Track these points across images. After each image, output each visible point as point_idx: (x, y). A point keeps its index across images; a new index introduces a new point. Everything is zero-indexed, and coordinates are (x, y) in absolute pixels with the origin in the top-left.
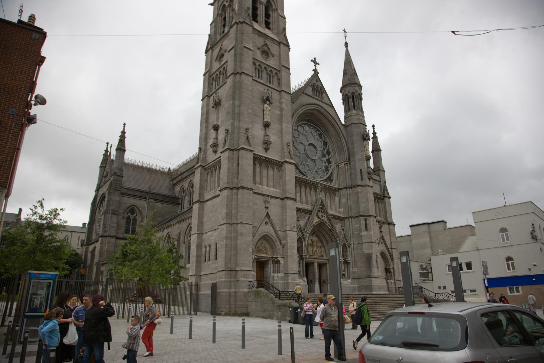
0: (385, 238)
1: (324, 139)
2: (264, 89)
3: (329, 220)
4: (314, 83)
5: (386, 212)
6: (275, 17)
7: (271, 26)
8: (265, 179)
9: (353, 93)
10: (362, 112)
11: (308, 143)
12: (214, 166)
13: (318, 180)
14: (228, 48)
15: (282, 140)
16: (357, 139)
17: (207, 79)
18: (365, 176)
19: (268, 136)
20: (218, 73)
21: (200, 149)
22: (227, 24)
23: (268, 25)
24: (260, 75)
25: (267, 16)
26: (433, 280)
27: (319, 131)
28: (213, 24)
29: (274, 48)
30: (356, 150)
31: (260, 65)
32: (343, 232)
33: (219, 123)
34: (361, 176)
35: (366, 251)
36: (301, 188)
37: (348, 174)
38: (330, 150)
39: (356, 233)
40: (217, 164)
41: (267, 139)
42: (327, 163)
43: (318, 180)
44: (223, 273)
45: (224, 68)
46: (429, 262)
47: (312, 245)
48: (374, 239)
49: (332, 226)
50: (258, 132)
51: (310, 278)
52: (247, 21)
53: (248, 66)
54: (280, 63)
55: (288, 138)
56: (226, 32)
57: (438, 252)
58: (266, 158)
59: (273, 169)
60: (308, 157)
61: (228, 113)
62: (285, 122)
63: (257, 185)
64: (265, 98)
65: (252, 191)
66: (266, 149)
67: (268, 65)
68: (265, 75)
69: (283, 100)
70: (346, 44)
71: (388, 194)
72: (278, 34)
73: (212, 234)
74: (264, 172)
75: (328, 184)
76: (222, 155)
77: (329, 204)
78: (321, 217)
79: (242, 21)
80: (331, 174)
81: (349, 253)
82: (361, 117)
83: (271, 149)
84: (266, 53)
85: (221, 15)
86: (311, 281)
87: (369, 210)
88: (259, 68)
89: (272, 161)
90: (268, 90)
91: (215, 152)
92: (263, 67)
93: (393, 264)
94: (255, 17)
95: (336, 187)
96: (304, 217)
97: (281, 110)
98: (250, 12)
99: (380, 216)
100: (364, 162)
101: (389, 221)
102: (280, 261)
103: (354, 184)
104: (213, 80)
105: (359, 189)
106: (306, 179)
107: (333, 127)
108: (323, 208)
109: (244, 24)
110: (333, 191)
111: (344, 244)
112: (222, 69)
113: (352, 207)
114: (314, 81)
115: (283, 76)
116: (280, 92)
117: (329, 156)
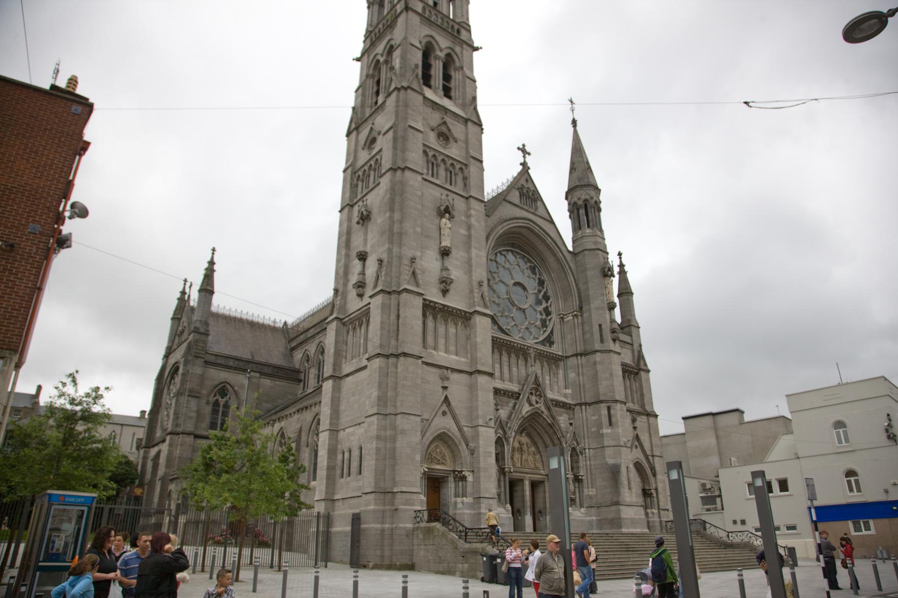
0: (642, 438)
1: (540, 275)
2: (442, 194)
3: (548, 409)
4: (522, 185)
5: (642, 395)
6: (459, 80)
7: (452, 94)
8: (442, 341)
9: (586, 200)
10: (601, 230)
11: (513, 282)
12: (359, 318)
13: (529, 342)
14: (384, 127)
15: (470, 276)
16: (593, 274)
17: (349, 177)
18: (608, 336)
19: (448, 270)
20: (366, 168)
21: (336, 291)
22: (382, 90)
23: (447, 92)
24: (435, 172)
25: (447, 77)
26: (723, 509)
27: (530, 261)
28: (360, 91)
29: (457, 129)
30: (591, 292)
31: (434, 156)
32: (571, 428)
33: (368, 249)
34: (601, 335)
35: (610, 461)
36: (501, 355)
37: (578, 333)
38: (550, 293)
39: (593, 429)
40: (364, 316)
41: (445, 275)
42: (544, 315)
43: (530, 342)
44: (371, 496)
45: (377, 160)
46: (716, 479)
47: (521, 450)
48: (623, 440)
49: (553, 418)
50: (430, 263)
51: (517, 505)
52: (415, 85)
53: (415, 158)
54: (467, 152)
55: (480, 273)
56: (380, 102)
57: (731, 462)
58: (444, 306)
59: (456, 324)
60: (513, 304)
61: (382, 233)
62: (475, 248)
63: (429, 350)
64: (442, 208)
65: (420, 361)
66: (445, 292)
67: (447, 156)
68: (442, 172)
69: (473, 212)
70: (574, 122)
71: (646, 365)
72: (463, 106)
73: (354, 431)
74: (441, 330)
75: (546, 349)
76: (372, 301)
77: (547, 382)
78: (534, 403)
79: (405, 86)
80: (552, 332)
81: (581, 464)
82: (599, 240)
83: (452, 292)
84: (445, 136)
85: (373, 76)
86: (519, 511)
87: (614, 392)
88: (432, 160)
89: (455, 311)
90: (447, 195)
91: (361, 296)
92: (440, 158)
93: (656, 483)
94: (427, 79)
95: (560, 353)
96: (507, 403)
97: (469, 227)
98: (420, 71)
99: (633, 403)
100: (606, 313)
101: (648, 410)
102: (466, 477)
103: (589, 348)
104: (358, 180)
105: (598, 357)
106: (509, 341)
107: (555, 255)
108: (538, 388)
109: (409, 91)
110: (553, 361)
111: (574, 449)
112: (372, 162)
113: (587, 387)
114: (523, 181)
115: (471, 174)
116: (467, 198)
117: (547, 302)
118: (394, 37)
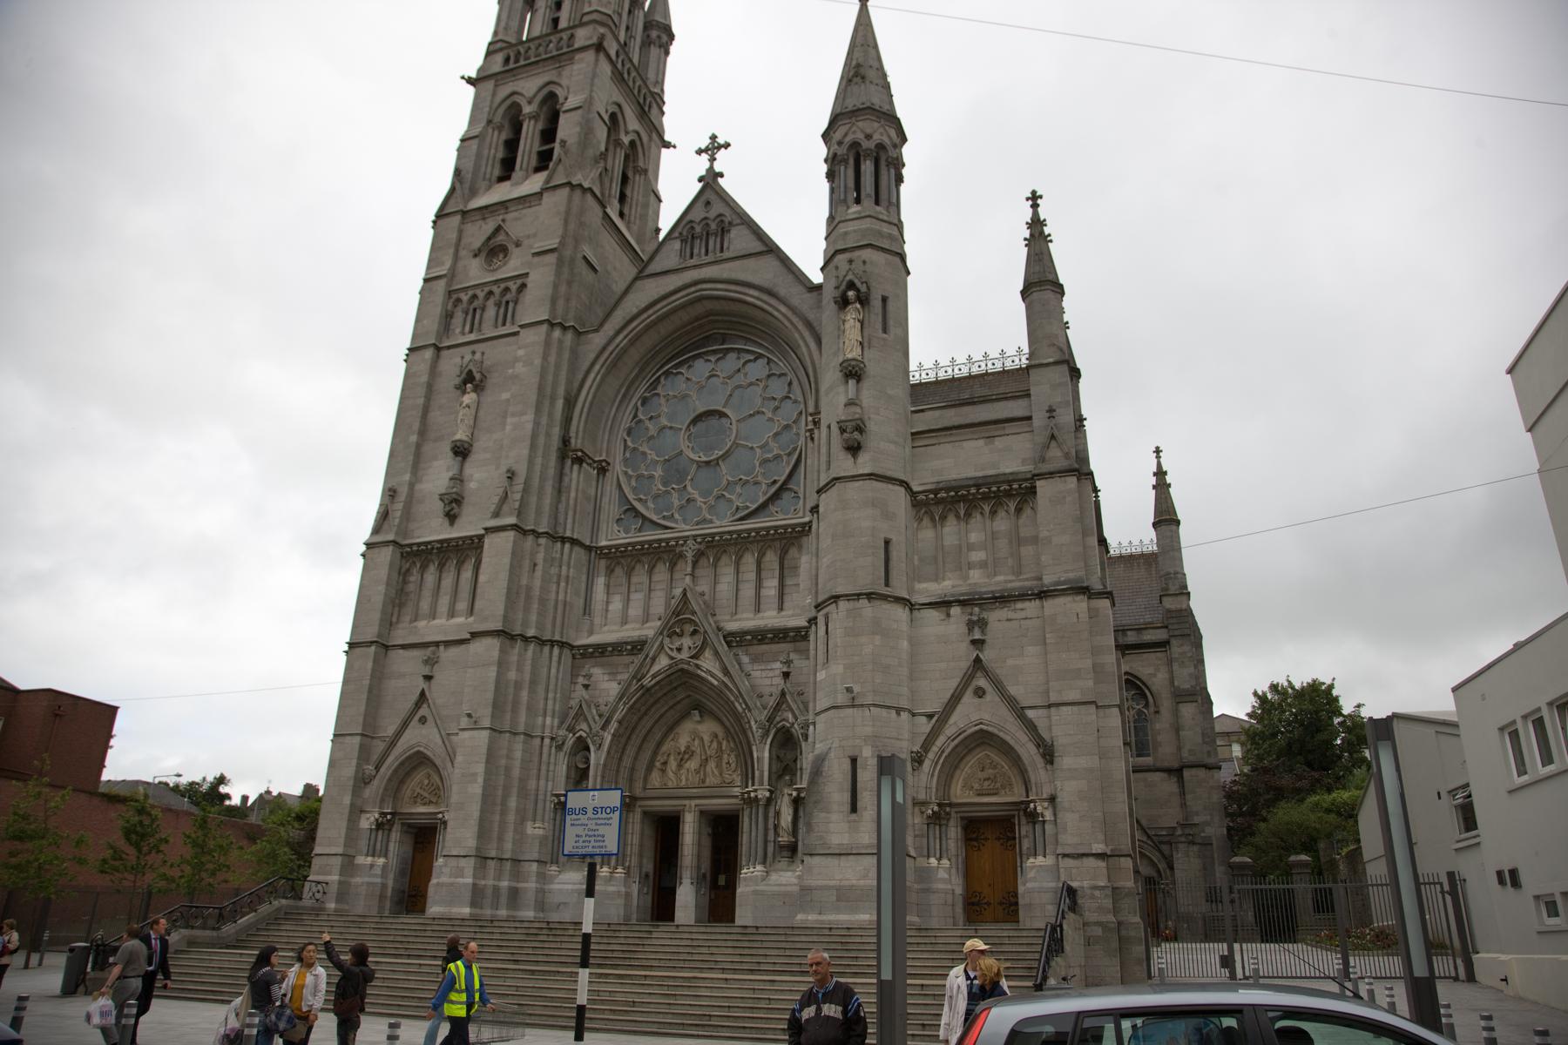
89: (461, 543)
91: (452, 517)
118: (564, 82)
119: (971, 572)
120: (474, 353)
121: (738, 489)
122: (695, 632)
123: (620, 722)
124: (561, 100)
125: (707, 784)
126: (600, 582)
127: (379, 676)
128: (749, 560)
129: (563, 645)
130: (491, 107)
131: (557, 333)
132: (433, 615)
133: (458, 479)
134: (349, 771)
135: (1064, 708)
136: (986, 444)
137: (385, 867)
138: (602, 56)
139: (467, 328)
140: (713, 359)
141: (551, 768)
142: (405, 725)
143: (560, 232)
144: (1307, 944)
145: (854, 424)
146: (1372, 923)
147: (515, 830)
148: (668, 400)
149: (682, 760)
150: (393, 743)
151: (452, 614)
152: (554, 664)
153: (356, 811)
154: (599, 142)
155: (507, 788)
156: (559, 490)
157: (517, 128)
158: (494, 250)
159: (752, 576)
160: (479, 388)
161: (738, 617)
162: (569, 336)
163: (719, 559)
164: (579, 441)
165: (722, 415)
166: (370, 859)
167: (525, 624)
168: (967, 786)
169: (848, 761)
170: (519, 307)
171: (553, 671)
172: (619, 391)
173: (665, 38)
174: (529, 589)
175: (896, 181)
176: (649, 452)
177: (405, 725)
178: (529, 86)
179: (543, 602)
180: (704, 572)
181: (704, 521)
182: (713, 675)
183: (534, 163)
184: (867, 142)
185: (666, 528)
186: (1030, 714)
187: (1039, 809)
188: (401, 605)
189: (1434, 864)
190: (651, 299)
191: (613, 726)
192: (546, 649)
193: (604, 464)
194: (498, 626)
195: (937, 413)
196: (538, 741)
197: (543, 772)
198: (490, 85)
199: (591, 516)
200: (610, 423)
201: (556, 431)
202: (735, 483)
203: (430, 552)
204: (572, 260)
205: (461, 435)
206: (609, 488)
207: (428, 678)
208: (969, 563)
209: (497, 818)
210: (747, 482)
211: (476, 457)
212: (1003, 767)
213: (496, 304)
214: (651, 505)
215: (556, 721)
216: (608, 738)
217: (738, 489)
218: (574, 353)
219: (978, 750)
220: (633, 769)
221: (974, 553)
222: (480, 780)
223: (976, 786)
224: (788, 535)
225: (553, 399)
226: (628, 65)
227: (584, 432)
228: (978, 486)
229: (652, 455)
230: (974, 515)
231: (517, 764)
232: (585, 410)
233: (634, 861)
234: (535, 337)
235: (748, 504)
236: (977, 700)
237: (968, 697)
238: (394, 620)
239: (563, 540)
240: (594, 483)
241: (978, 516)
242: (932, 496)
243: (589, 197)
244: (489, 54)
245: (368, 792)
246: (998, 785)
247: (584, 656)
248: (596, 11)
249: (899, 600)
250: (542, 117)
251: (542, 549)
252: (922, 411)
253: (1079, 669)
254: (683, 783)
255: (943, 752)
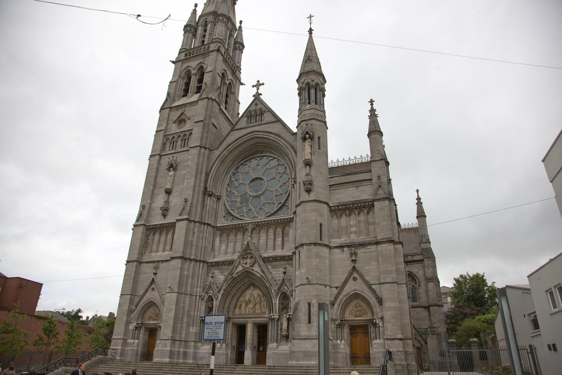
89: (168, 225)
91: (164, 216)
118: (206, 62)
119: (351, 235)
120: (173, 157)
121: (267, 206)
122: (251, 257)
123: (224, 290)
124: (205, 69)
125: (256, 313)
126: (218, 239)
127: (137, 273)
128: (271, 231)
129: (204, 262)
130: (180, 71)
131: (203, 150)
132: (157, 251)
133: (167, 202)
134: (126, 308)
135: (386, 285)
136: (356, 189)
137: (138, 343)
138: (219, 53)
139: (171, 148)
140: (258, 159)
141: (199, 307)
142: (146, 291)
143: (204, 115)
144: (478, 372)
145: (308, 182)
146: (502, 364)
147: (186, 330)
148: (242, 174)
149: (247, 304)
150: (142, 298)
151: (164, 250)
152: (201, 269)
153: (128, 323)
154: (218, 83)
155: (183, 315)
156: (203, 206)
157: (189, 79)
158: (181, 121)
159: (272, 237)
160: (175, 170)
161: (267, 252)
162: (207, 151)
163: (260, 231)
164: (210, 188)
165: (261, 179)
166: (133, 341)
167: (191, 254)
168: (351, 313)
169: (307, 304)
170: (189, 141)
171: (200, 271)
172: (225, 170)
173: (241, 47)
174: (192, 241)
175: (323, 96)
176: (235, 192)
177: (146, 291)
178: (194, 64)
179: (197, 246)
180: (255, 235)
181: (255, 217)
182: (258, 273)
183: (195, 90)
184: (312, 83)
185: (242, 219)
186: (373, 287)
187: (377, 322)
188: (146, 247)
189: (524, 342)
190: (236, 138)
191: (222, 291)
192: (198, 263)
193: (219, 197)
194: (180, 255)
195: (338, 178)
196: (195, 297)
197: (196, 308)
198: (180, 63)
199: (215, 215)
200: (221, 182)
201: (202, 185)
202: (266, 203)
203: (156, 228)
204: (208, 125)
205: (168, 186)
206: (221, 205)
207: (155, 274)
208: (350, 232)
209: (179, 325)
210: (270, 203)
211: (174, 194)
212: (364, 306)
213: (181, 140)
214: (236, 211)
215: (201, 290)
216: (220, 296)
217: (267, 206)
218: (209, 157)
219: (355, 300)
220: (229, 308)
221: (352, 228)
222: (173, 311)
223: (354, 313)
224: (285, 222)
225: (201, 173)
226: (228, 57)
227: (212, 185)
228: (353, 204)
229: (236, 193)
230: (352, 214)
231: (187, 305)
232: (213, 177)
233: (229, 341)
234: (195, 151)
235: (271, 211)
236: (354, 282)
237: (351, 281)
238: (143, 253)
239: (204, 224)
240: (216, 203)
241: (354, 215)
242: (337, 208)
243: (214, 102)
244: (180, 53)
245: (133, 316)
246: (362, 313)
247: (211, 266)
248: (217, 38)
249: (325, 245)
250: (198, 74)
251: (197, 227)
252: (333, 177)
253: (391, 270)
254: (247, 312)
255: (342, 301)
